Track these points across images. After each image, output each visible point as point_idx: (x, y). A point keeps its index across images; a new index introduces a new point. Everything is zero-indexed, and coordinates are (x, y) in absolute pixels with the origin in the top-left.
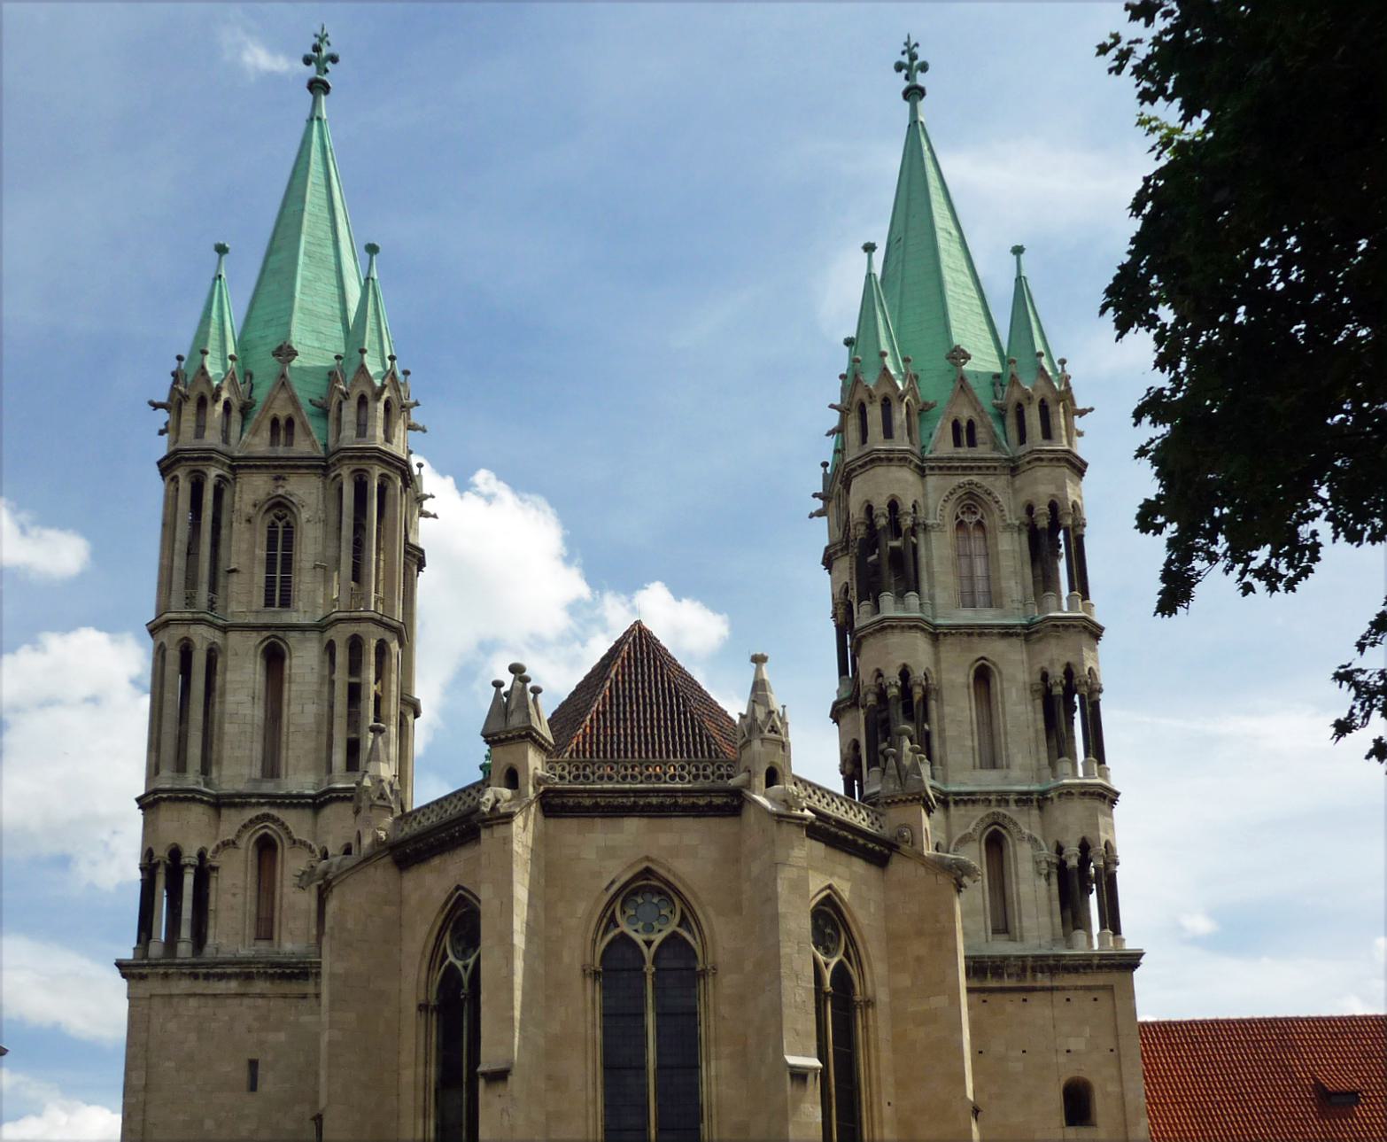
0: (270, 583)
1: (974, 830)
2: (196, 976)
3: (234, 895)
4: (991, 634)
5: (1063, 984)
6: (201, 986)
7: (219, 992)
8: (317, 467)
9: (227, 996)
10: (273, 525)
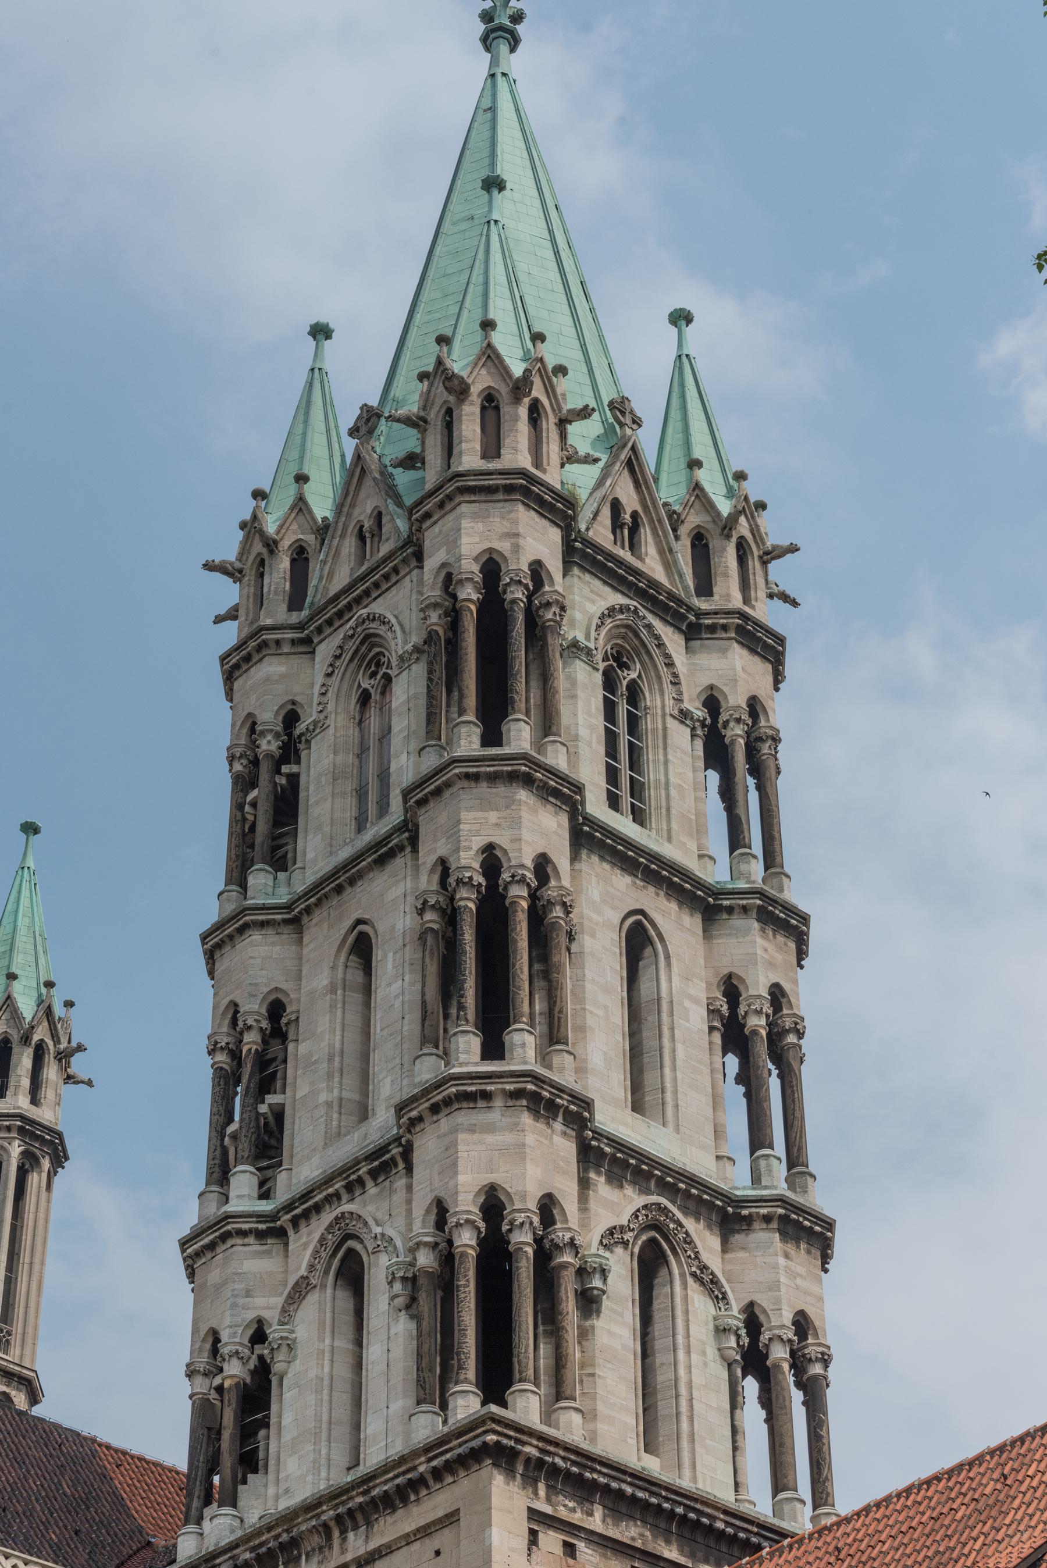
1: (311, 1267)
4: (360, 875)
5: (384, 1540)
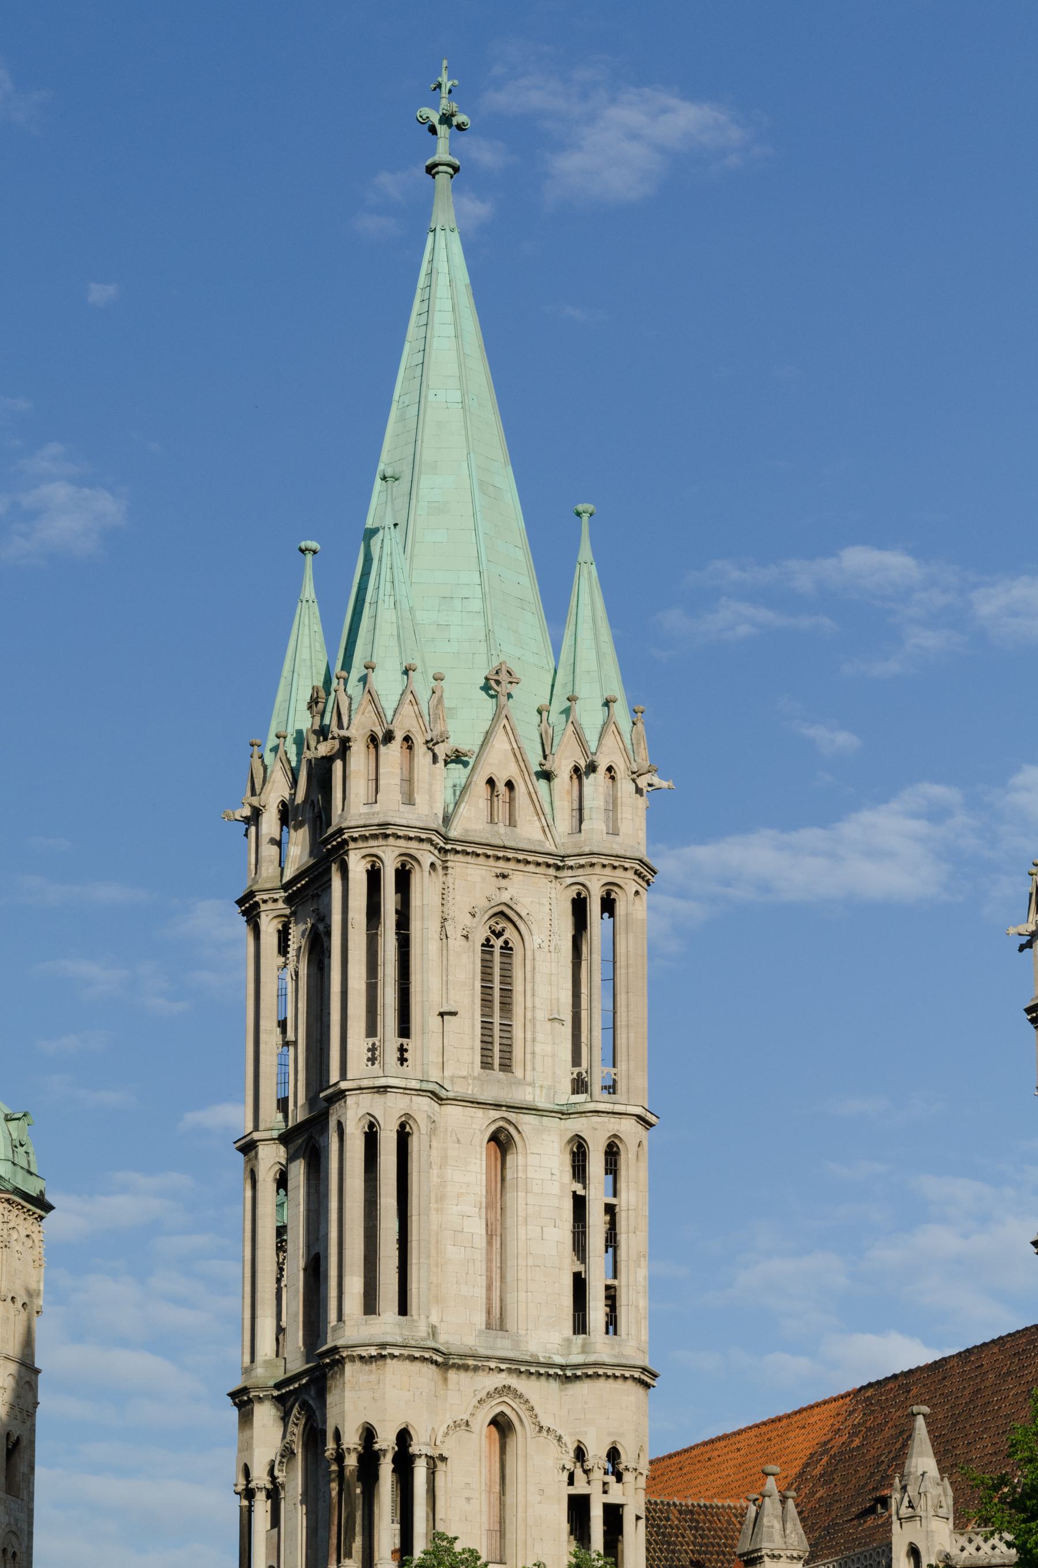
0: (487, 1026)
3: (468, 1499)
8: (548, 866)
10: (487, 944)
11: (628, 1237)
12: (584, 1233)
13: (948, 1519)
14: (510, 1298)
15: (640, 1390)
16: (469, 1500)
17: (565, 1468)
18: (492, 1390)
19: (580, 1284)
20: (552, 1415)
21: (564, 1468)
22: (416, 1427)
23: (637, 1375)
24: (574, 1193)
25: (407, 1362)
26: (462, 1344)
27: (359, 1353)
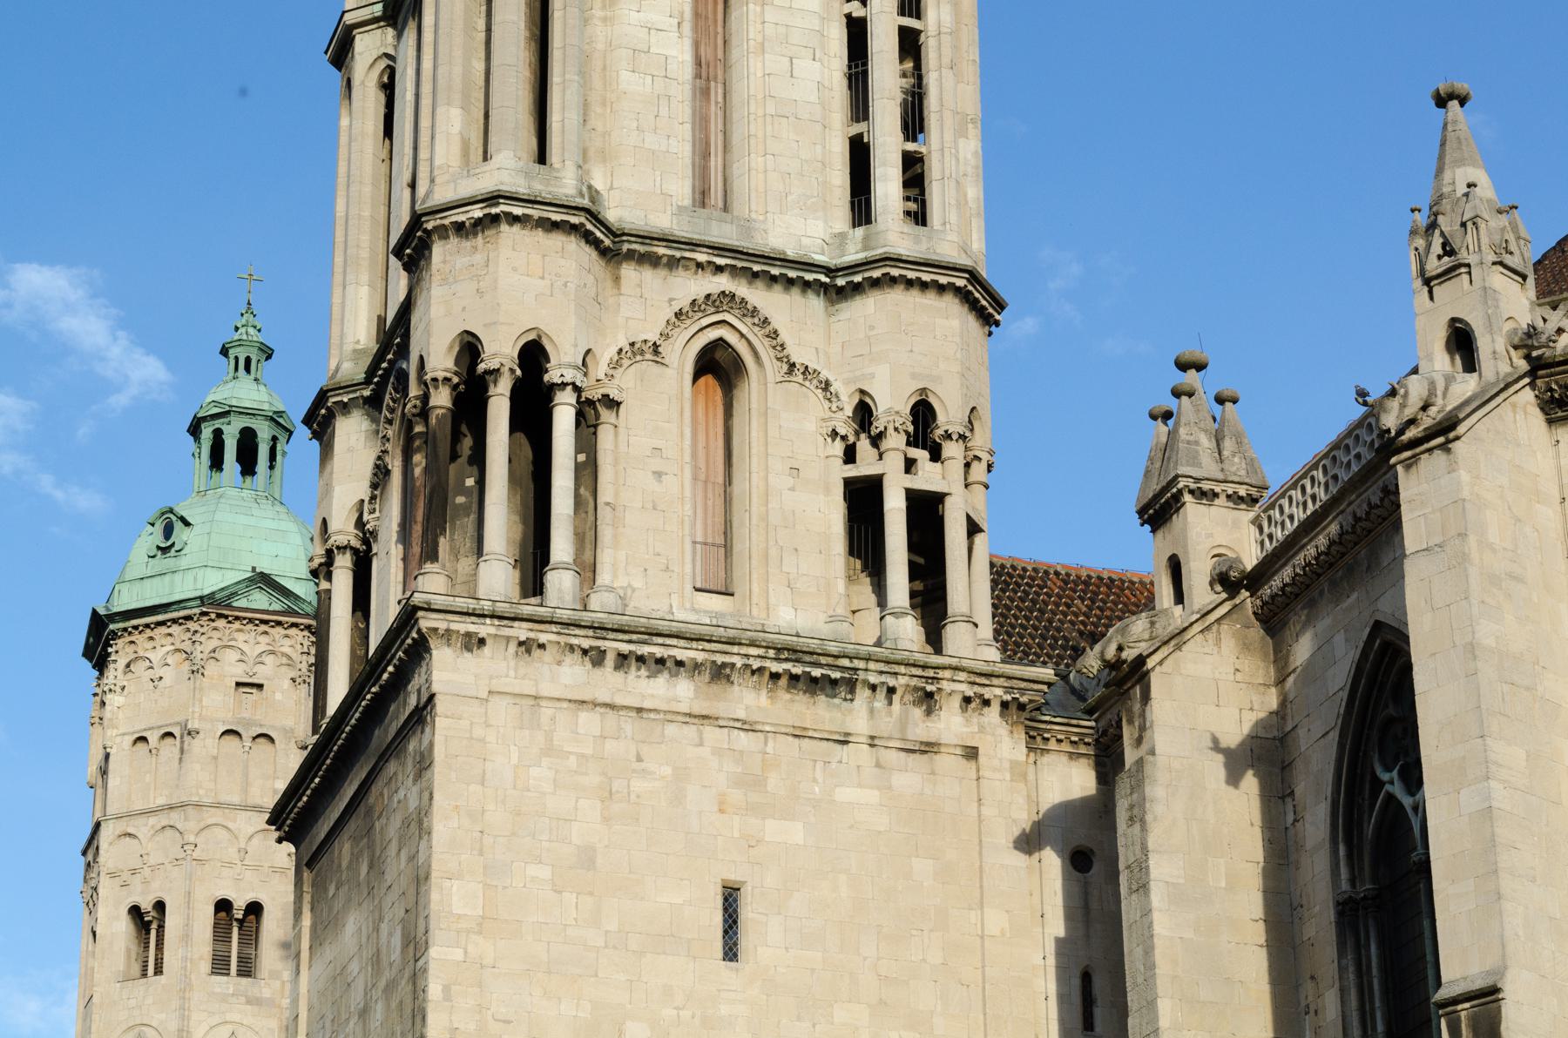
2: (596, 657)
6: (609, 683)
7: (646, 705)
9: (671, 716)
11: (941, 76)
12: (865, 73)
13: (1524, 277)
14: (736, 170)
15: (972, 322)
16: (660, 477)
17: (837, 434)
18: (701, 298)
19: (860, 154)
20: (814, 350)
21: (834, 434)
22: (554, 338)
23: (960, 283)
24: (849, 17)
25: (540, 232)
26: (646, 225)
27: (454, 219)
